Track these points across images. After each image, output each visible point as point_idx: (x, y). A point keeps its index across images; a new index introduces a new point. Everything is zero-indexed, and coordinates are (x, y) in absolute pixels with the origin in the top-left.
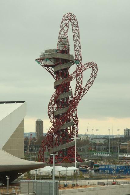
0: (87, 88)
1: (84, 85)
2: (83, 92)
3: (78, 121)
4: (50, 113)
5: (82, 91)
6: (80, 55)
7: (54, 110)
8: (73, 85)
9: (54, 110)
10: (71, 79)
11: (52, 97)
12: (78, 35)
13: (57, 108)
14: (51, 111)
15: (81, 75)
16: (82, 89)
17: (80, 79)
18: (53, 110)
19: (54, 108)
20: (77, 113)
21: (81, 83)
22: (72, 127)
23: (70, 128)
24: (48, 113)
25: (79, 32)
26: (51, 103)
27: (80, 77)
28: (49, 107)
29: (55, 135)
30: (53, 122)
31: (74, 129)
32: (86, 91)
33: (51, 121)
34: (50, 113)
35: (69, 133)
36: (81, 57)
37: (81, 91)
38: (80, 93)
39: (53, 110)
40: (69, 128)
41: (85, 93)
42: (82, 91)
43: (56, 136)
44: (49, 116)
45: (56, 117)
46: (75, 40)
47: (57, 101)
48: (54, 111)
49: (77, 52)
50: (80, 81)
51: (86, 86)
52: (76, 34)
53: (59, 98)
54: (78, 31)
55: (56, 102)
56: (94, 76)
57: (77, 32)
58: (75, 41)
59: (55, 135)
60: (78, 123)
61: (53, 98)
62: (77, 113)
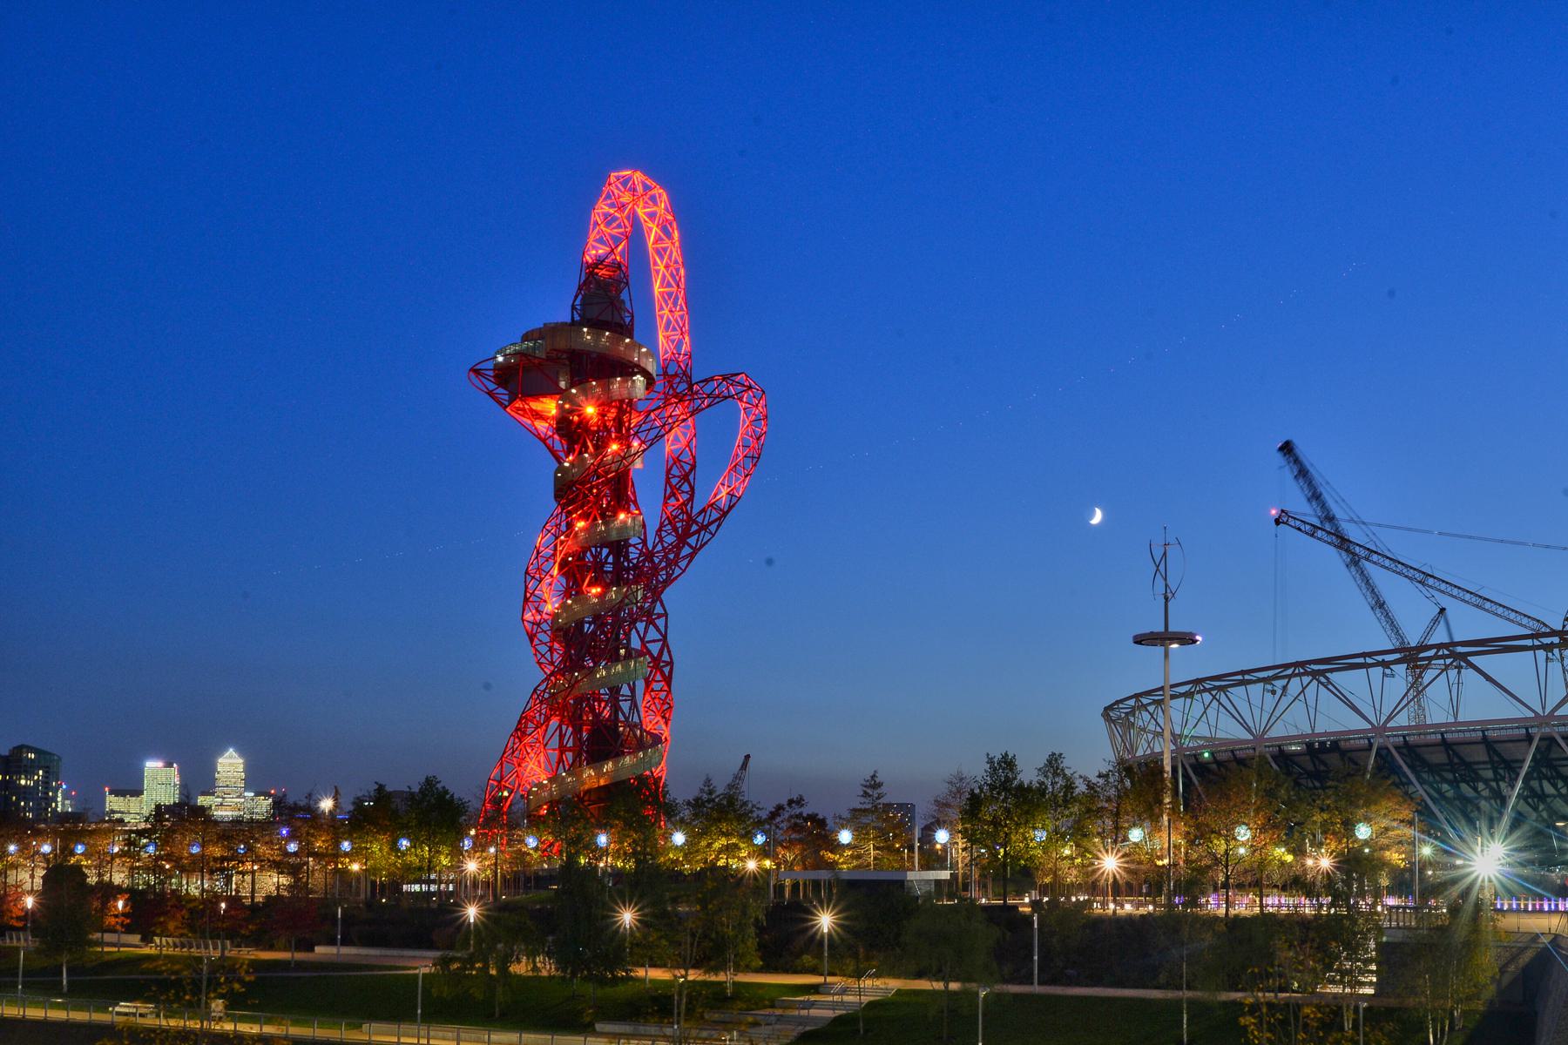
2: (698, 532)
3: (671, 663)
5: (694, 528)
16: (691, 520)
23: (633, 690)
30: (552, 663)
32: (713, 528)
33: (543, 660)
35: (624, 714)
38: (682, 539)
42: (694, 528)
43: (560, 727)
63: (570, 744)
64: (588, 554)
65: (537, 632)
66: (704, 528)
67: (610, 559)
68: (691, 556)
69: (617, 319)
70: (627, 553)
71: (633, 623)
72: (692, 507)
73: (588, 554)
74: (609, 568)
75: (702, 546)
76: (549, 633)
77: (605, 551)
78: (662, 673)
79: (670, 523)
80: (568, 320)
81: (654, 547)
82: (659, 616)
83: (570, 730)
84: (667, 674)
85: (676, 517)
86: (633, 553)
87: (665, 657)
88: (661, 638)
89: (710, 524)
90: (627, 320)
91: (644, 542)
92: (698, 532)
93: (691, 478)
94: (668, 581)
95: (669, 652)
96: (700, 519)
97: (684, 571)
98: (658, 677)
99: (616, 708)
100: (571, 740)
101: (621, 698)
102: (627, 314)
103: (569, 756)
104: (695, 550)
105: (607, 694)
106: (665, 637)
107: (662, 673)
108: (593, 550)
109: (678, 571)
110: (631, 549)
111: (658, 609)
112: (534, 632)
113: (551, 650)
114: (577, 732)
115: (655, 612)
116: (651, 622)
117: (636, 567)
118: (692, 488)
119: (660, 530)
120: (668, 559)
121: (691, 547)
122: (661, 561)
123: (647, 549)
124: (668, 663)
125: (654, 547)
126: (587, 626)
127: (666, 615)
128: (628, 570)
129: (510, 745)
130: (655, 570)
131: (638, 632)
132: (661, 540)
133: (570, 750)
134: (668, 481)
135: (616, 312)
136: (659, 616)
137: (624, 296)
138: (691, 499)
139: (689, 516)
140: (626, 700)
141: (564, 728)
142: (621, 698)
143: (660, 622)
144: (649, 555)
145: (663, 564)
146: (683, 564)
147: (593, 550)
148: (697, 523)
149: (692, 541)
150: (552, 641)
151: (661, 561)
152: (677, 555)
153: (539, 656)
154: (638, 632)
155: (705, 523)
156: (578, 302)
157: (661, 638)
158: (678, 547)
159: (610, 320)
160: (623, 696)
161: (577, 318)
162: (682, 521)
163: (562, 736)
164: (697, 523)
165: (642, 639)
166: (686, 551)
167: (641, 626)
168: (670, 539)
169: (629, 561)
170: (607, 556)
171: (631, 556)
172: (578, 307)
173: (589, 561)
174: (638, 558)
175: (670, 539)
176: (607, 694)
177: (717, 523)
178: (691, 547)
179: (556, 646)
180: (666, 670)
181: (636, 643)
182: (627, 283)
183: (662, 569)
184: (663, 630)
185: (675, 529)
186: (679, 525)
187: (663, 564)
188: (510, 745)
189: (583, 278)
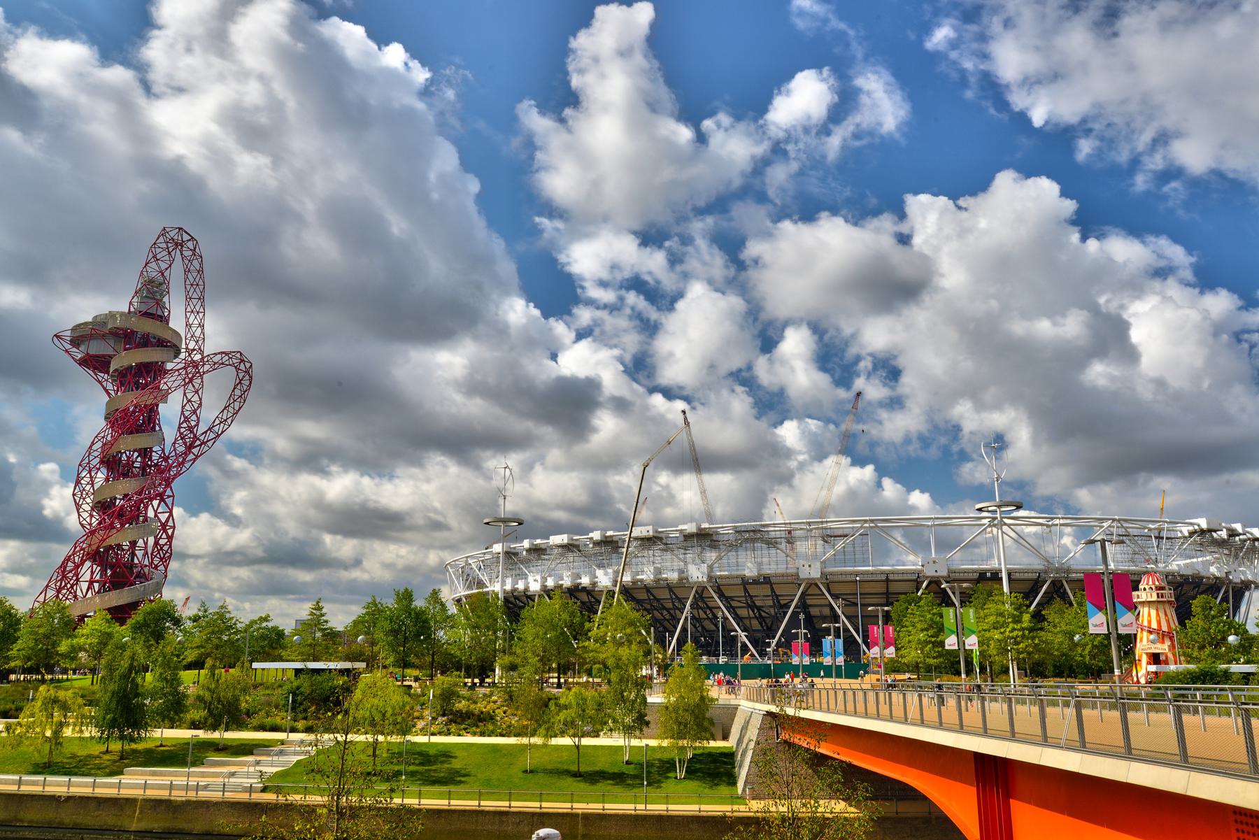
0: (212, 436)
1: (202, 428)
2: (200, 445)
3: (174, 527)
5: (198, 443)
7: (96, 487)
9: (96, 487)
10: (164, 398)
12: (200, 271)
13: (107, 480)
14: (84, 490)
16: (196, 438)
18: (93, 485)
19: (97, 480)
22: (151, 540)
23: (146, 544)
25: (201, 264)
26: (89, 463)
29: (88, 564)
30: (90, 524)
31: (159, 553)
32: (210, 444)
33: (84, 522)
38: (189, 448)
40: (141, 543)
41: (206, 448)
42: (198, 443)
46: (188, 282)
49: (192, 317)
50: (196, 398)
51: (210, 429)
52: (192, 268)
53: (114, 451)
54: (200, 260)
57: (196, 263)
60: (173, 533)
61: (99, 444)
66: (203, 443)
68: (194, 460)
69: (159, 313)
70: (151, 456)
71: (151, 499)
75: (201, 454)
77: (136, 454)
78: (167, 534)
79: (182, 439)
80: (127, 311)
81: (170, 454)
82: (169, 497)
83: (99, 568)
86: (155, 457)
87: (170, 523)
89: (208, 441)
90: (166, 314)
91: (163, 450)
92: (200, 445)
93: (198, 412)
94: (178, 474)
95: (173, 520)
96: (202, 438)
98: (164, 536)
99: (133, 554)
103: (96, 585)
104: (197, 457)
107: (167, 534)
108: (128, 453)
109: (184, 469)
110: (154, 454)
111: (168, 492)
113: (91, 516)
114: (103, 572)
116: (162, 500)
117: (156, 465)
118: (198, 419)
119: (174, 443)
120: (178, 461)
122: (173, 463)
123: (164, 454)
124: (171, 527)
125: (170, 454)
126: (118, 501)
127: (173, 496)
128: (150, 466)
129: (54, 577)
130: (169, 468)
131: (153, 506)
132: (175, 450)
133: (97, 581)
134: (182, 413)
136: (169, 497)
137: (166, 299)
138: (197, 425)
139: (195, 436)
141: (95, 566)
144: (166, 459)
145: (175, 464)
146: (187, 465)
147: (128, 453)
148: (199, 440)
149: (195, 451)
150: (92, 509)
151: (173, 463)
152: (184, 459)
154: (153, 506)
158: (185, 454)
163: (92, 573)
164: (199, 440)
165: (156, 512)
166: (191, 456)
167: (155, 503)
168: (182, 449)
169: (152, 461)
170: (137, 457)
171: (153, 458)
175: (182, 449)
179: (94, 514)
180: (170, 532)
181: (151, 513)
182: (168, 292)
183: (174, 467)
185: (185, 443)
186: (188, 440)
187: (175, 464)
188: (54, 577)
189: (139, 286)
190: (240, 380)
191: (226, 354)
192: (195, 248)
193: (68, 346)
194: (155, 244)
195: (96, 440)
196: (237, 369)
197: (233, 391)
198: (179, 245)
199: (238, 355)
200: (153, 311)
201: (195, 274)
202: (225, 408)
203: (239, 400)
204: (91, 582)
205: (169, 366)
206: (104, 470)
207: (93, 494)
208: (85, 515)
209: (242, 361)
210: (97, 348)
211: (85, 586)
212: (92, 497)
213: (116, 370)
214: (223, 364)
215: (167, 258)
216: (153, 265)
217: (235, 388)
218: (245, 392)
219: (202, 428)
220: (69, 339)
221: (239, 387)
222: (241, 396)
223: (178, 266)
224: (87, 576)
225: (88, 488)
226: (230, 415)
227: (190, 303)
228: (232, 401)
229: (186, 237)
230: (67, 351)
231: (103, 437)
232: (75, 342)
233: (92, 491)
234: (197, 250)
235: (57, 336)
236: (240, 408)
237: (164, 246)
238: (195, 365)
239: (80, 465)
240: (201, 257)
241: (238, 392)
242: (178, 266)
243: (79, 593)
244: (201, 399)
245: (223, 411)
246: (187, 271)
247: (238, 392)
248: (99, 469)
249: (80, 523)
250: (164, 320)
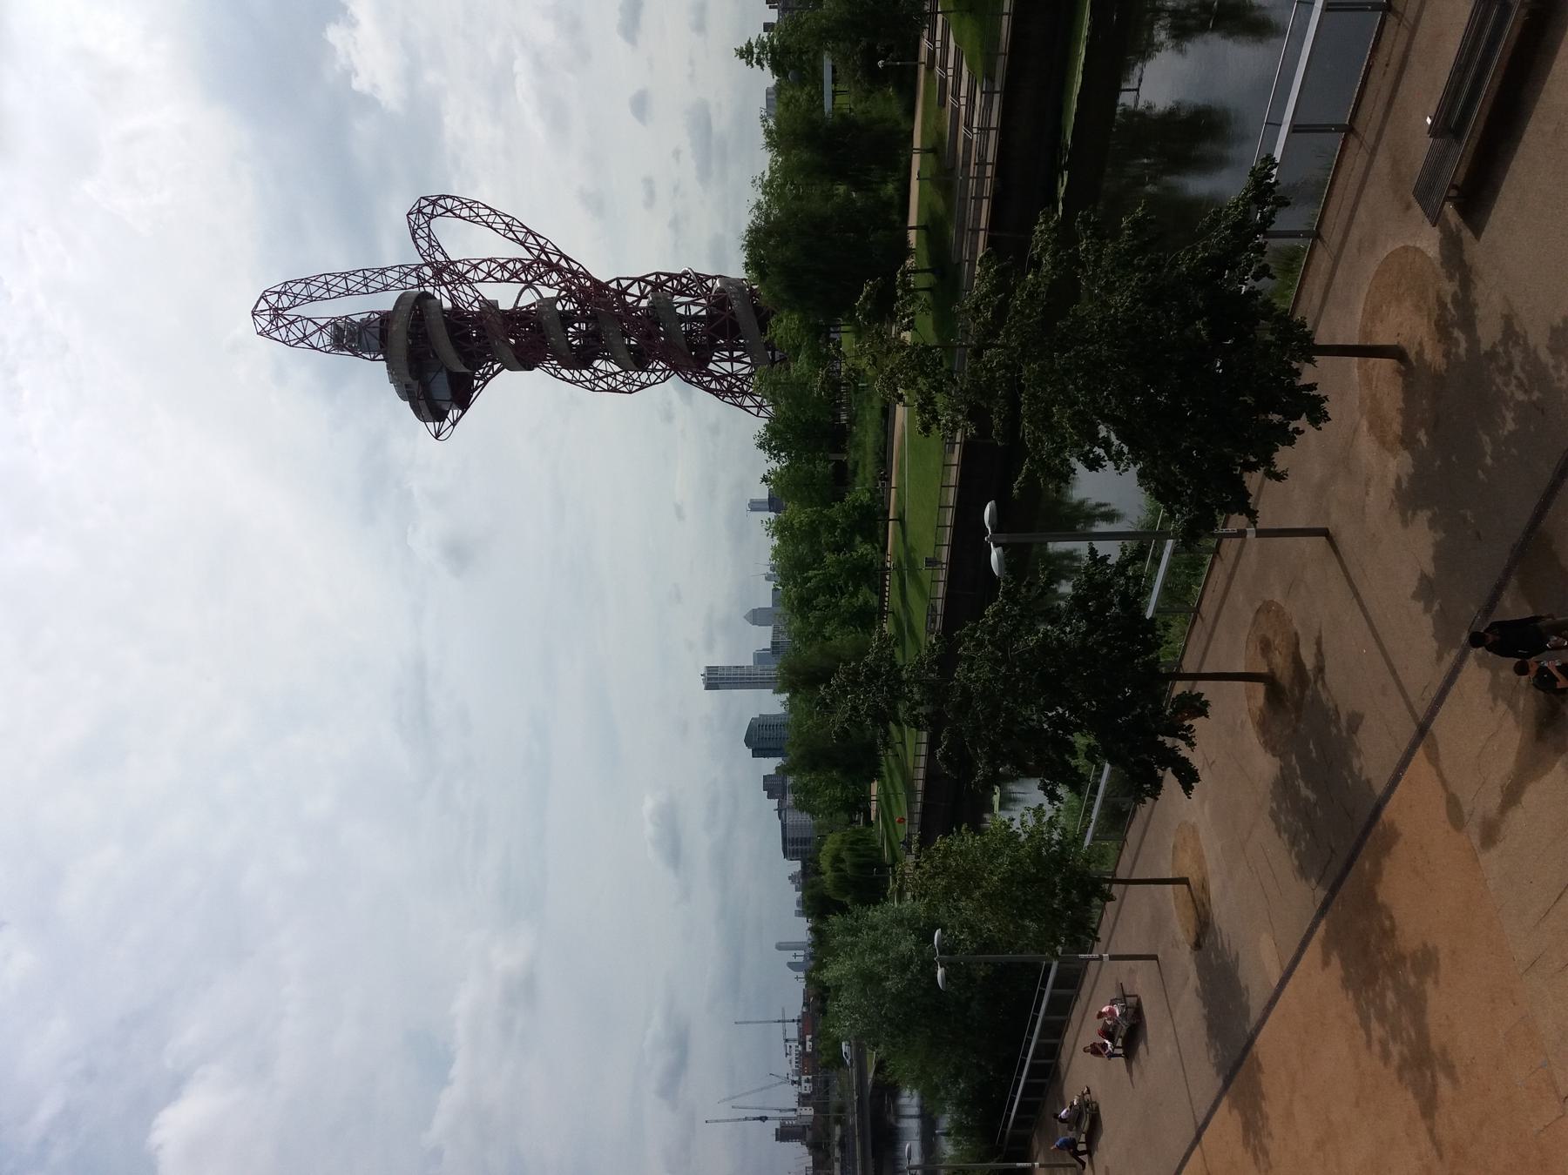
0: (531, 240)
1: (522, 253)
3: (658, 274)
4: (630, 384)
5: (543, 257)
6: (383, 272)
7: (617, 369)
8: (505, 296)
10: (493, 305)
11: (564, 379)
12: (307, 282)
13: (607, 359)
14: (623, 382)
15: (460, 266)
16: (538, 260)
17: (476, 267)
18: (615, 374)
19: (609, 370)
20: (628, 279)
21: (489, 262)
22: (677, 299)
23: (681, 304)
24: (630, 392)
25: (296, 282)
26: (590, 381)
27: (467, 268)
28: (608, 391)
29: (711, 366)
30: (664, 370)
31: (691, 288)
32: (542, 242)
33: (662, 377)
34: (630, 384)
36: (392, 268)
37: (542, 261)
38: (552, 267)
39: (618, 373)
40: (681, 310)
41: (549, 245)
42: (543, 257)
43: (714, 362)
44: (642, 388)
45: (639, 360)
46: (327, 296)
47: (579, 359)
48: (620, 370)
50: (484, 266)
51: (522, 243)
54: (291, 284)
55: (587, 366)
56: (471, 212)
57: (297, 289)
58: (333, 294)
59: (711, 366)
60: (664, 274)
61: (565, 372)
62: (628, 279)
63: (727, 353)
64: (574, 343)
65: (640, 382)
66: (542, 249)
67: (577, 325)
68: (567, 259)
69: (377, 324)
70: (570, 311)
72: (527, 260)
73: (574, 343)
74: (583, 326)
75: (558, 251)
76: (640, 373)
77: (571, 329)
78: (667, 281)
82: (619, 284)
83: (716, 354)
84: (666, 277)
85: (536, 273)
87: (652, 278)
88: (637, 283)
89: (539, 244)
90: (377, 316)
93: (501, 261)
94: (587, 276)
96: (536, 253)
97: (581, 265)
98: (670, 284)
99: (696, 318)
100: (724, 353)
101: (688, 314)
102: (372, 316)
104: (562, 256)
105: (685, 326)
106: (636, 280)
107: (667, 281)
108: (570, 339)
109: (581, 270)
110: (567, 308)
111: (614, 285)
112: (640, 384)
113: (654, 371)
114: (720, 349)
115: (616, 288)
121: (560, 260)
126: (632, 343)
127: (618, 279)
130: (582, 288)
133: (731, 354)
134: (508, 281)
135: (371, 325)
136: (619, 284)
137: (357, 319)
138: (520, 260)
139: (534, 262)
140: (690, 310)
141: (714, 358)
142: (688, 314)
143: (625, 283)
146: (575, 267)
147: (570, 339)
149: (555, 259)
153: (659, 380)
155: (538, 248)
156: (368, 356)
157: (637, 283)
159: (377, 329)
160: (686, 312)
161: (381, 357)
162: (538, 268)
163: (722, 360)
166: (563, 263)
167: (629, 299)
169: (576, 309)
170: (574, 328)
171: (572, 308)
172: (372, 356)
173: (580, 342)
174: (573, 303)
175: (555, 276)
176: (685, 326)
177: (538, 238)
178: (560, 260)
179: (651, 367)
180: (663, 278)
182: (346, 317)
184: (631, 281)
185: (547, 273)
186: (542, 270)
190: (448, 211)
191: (414, 233)
192: (276, 293)
193: (447, 423)
194: (284, 342)
195: (559, 376)
196: (432, 216)
197: (464, 218)
198: (277, 313)
199: (413, 217)
200: (376, 331)
201: (313, 289)
202: (489, 226)
203: (476, 210)
204: (732, 360)
205: (447, 304)
206: (596, 363)
207: (627, 372)
208: (653, 377)
209: (420, 211)
210: (441, 388)
211: (737, 366)
212: (631, 373)
213: (466, 366)
214: (429, 236)
215: (299, 325)
216: (314, 340)
217: (460, 217)
218: (463, 203)
219: (522, 253)
220: (437, 424)
221: (457, 212)
222: (470, 208)
223: (306, 310)
224: (727, 366)
225: (620, 378)
226: (498, 220)
227: (354, 289)
228: (478, 219)
229: (263, 305)
230: (454, 424)
231: (555, 369)
232: (440, 416)
233: (623, 374)
234: (277, 289)
235: (437, 437)
236: (487, 207)
237: (283, 330)
238: (438, 273)
239: (593, 390)
240: (286, 283)
241: (465, 212)
242: (306, 310)
243: (746, 371)
244: (484, 260)
245: (495, 229)
246: (311, 298)
247: (465, 212)
248: (596, 369)
249: (663, 381)
250: (385, 318)
